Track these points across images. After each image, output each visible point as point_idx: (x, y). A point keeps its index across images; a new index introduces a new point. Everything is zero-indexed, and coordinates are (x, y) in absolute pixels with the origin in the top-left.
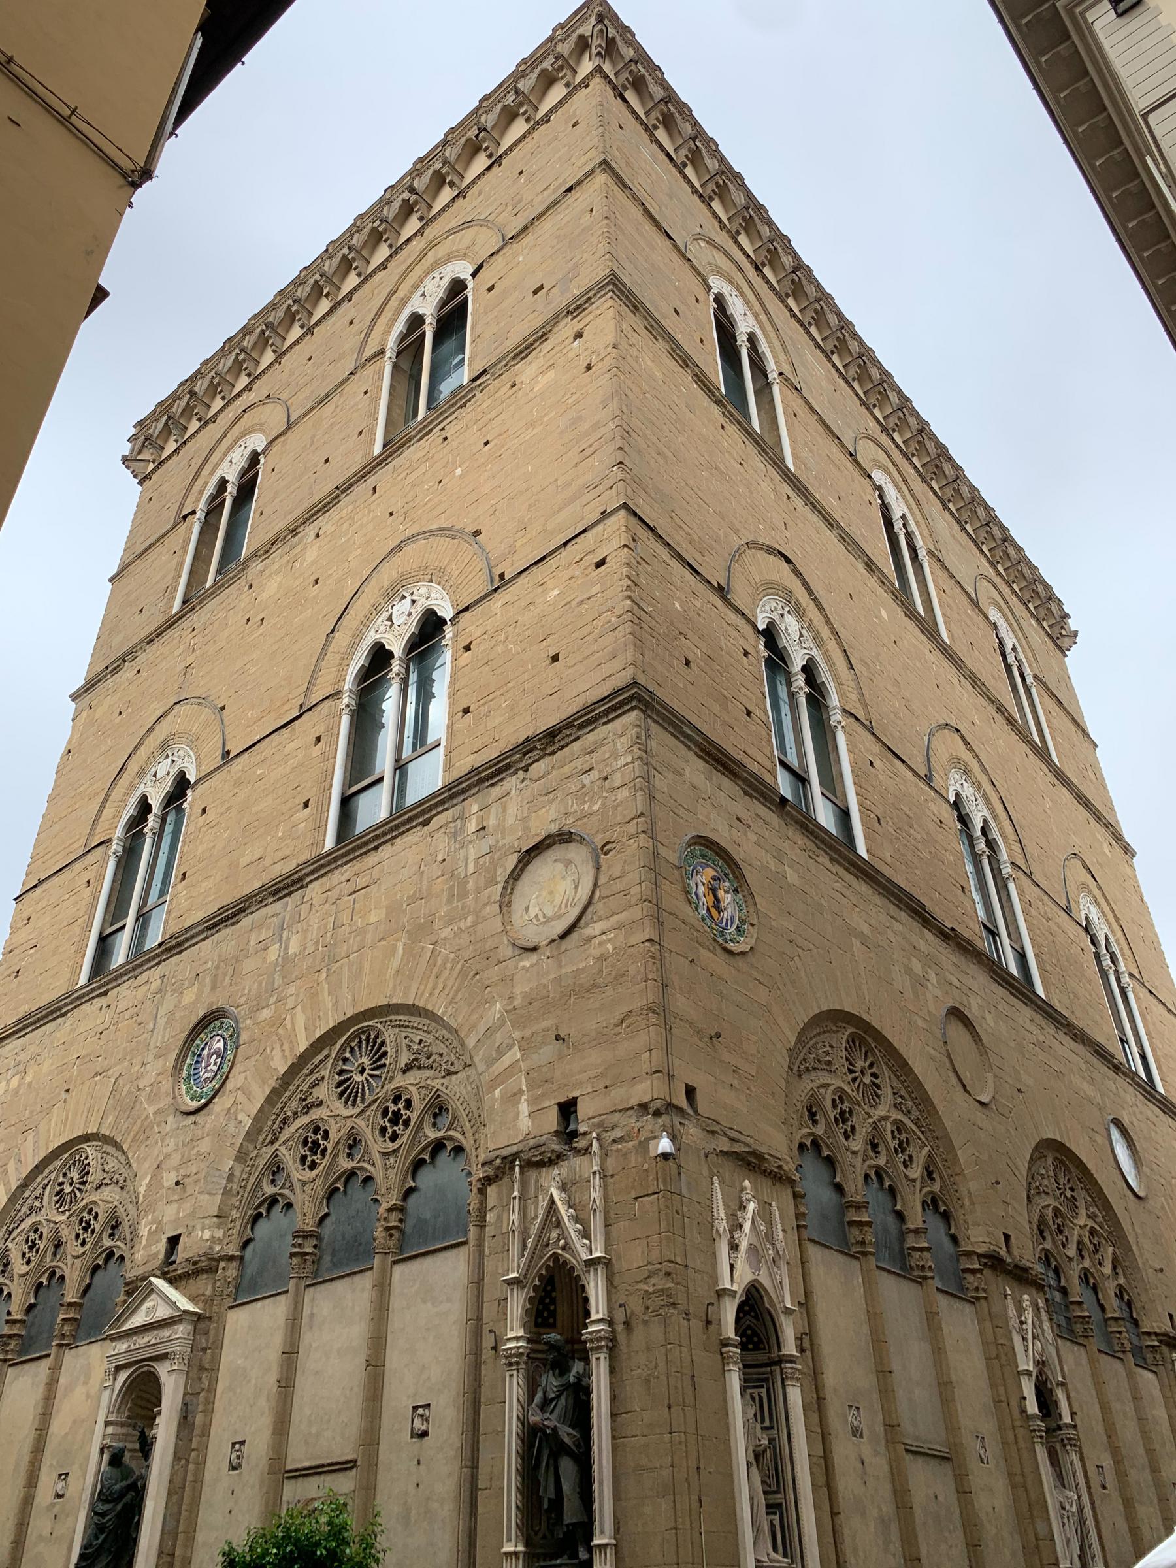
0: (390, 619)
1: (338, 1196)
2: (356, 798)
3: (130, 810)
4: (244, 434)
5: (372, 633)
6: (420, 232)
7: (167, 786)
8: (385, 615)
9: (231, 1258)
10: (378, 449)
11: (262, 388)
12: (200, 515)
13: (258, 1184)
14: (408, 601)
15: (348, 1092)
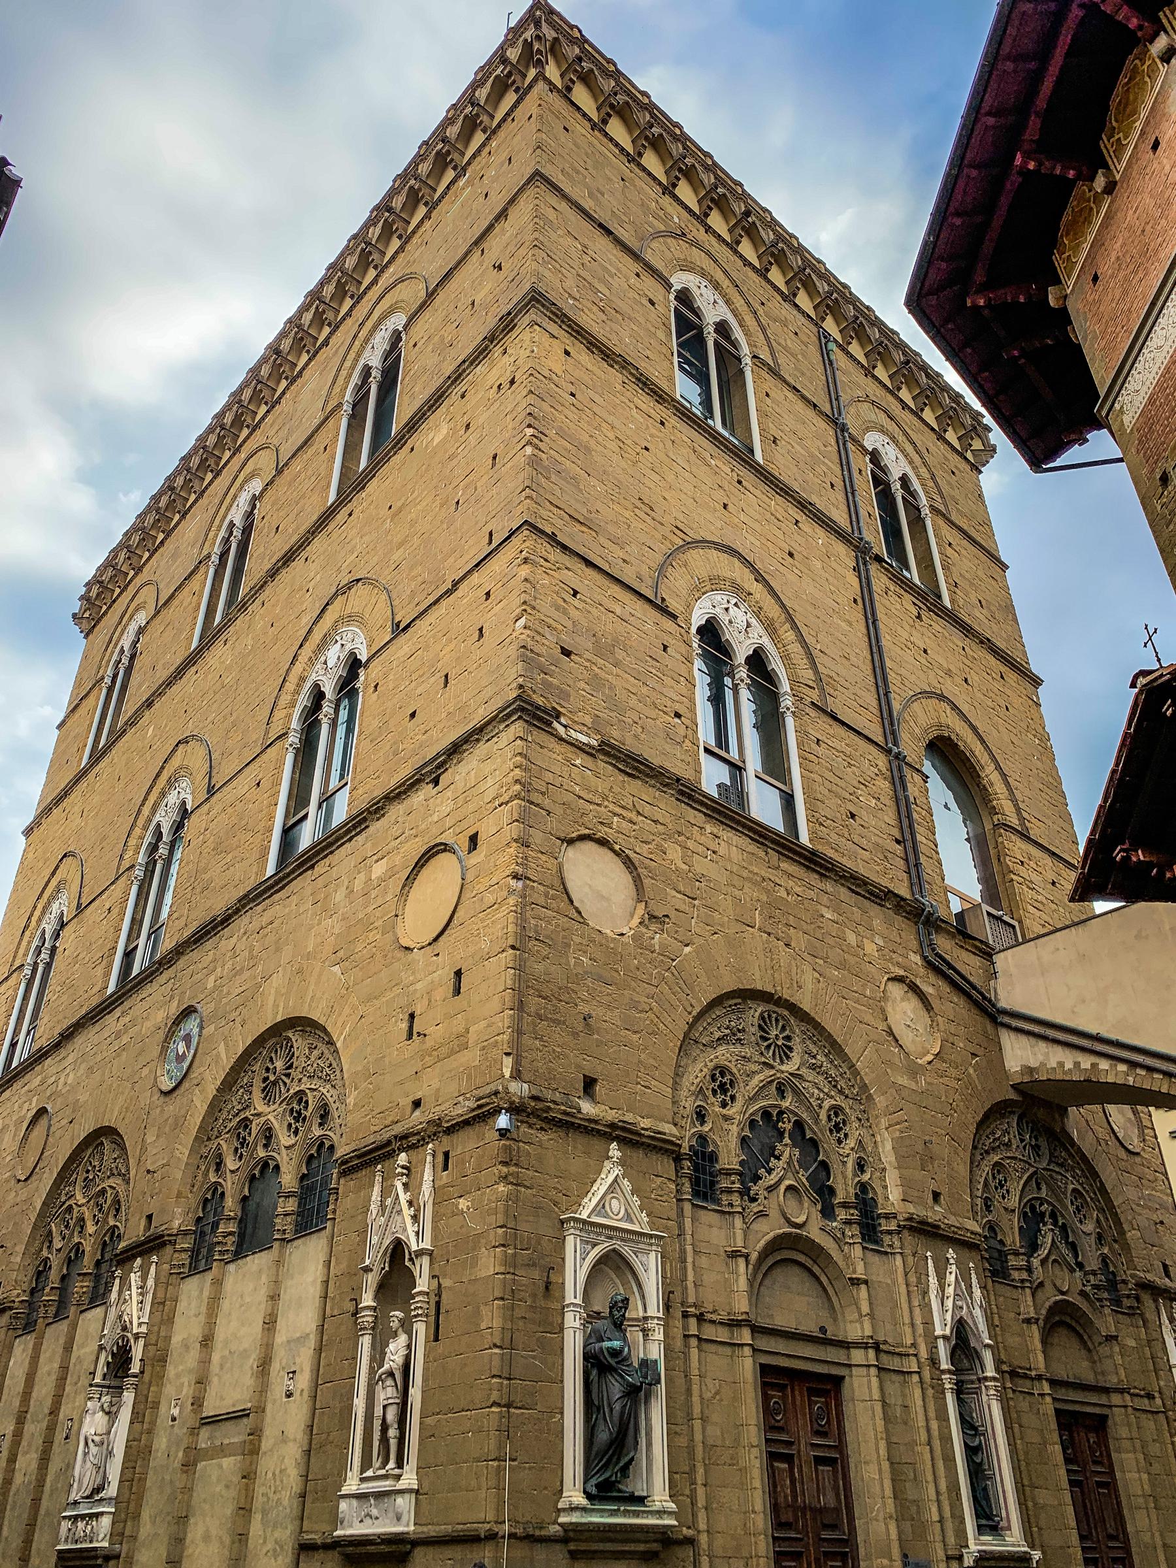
0: (325, 663)
1: (256, 1184)
2: (298, 828)
3: (149, 838)
4: (246, 481)
5: (314, 675)
6: (375, 282)
7: (174, 816)
8: (323, 659)
9: (186, 1233)
10: (332, 497)
11: (258, 439)
12: (215, 559)
13: (206, 1174)
14: (338, 645)
15: (269, 1091)
